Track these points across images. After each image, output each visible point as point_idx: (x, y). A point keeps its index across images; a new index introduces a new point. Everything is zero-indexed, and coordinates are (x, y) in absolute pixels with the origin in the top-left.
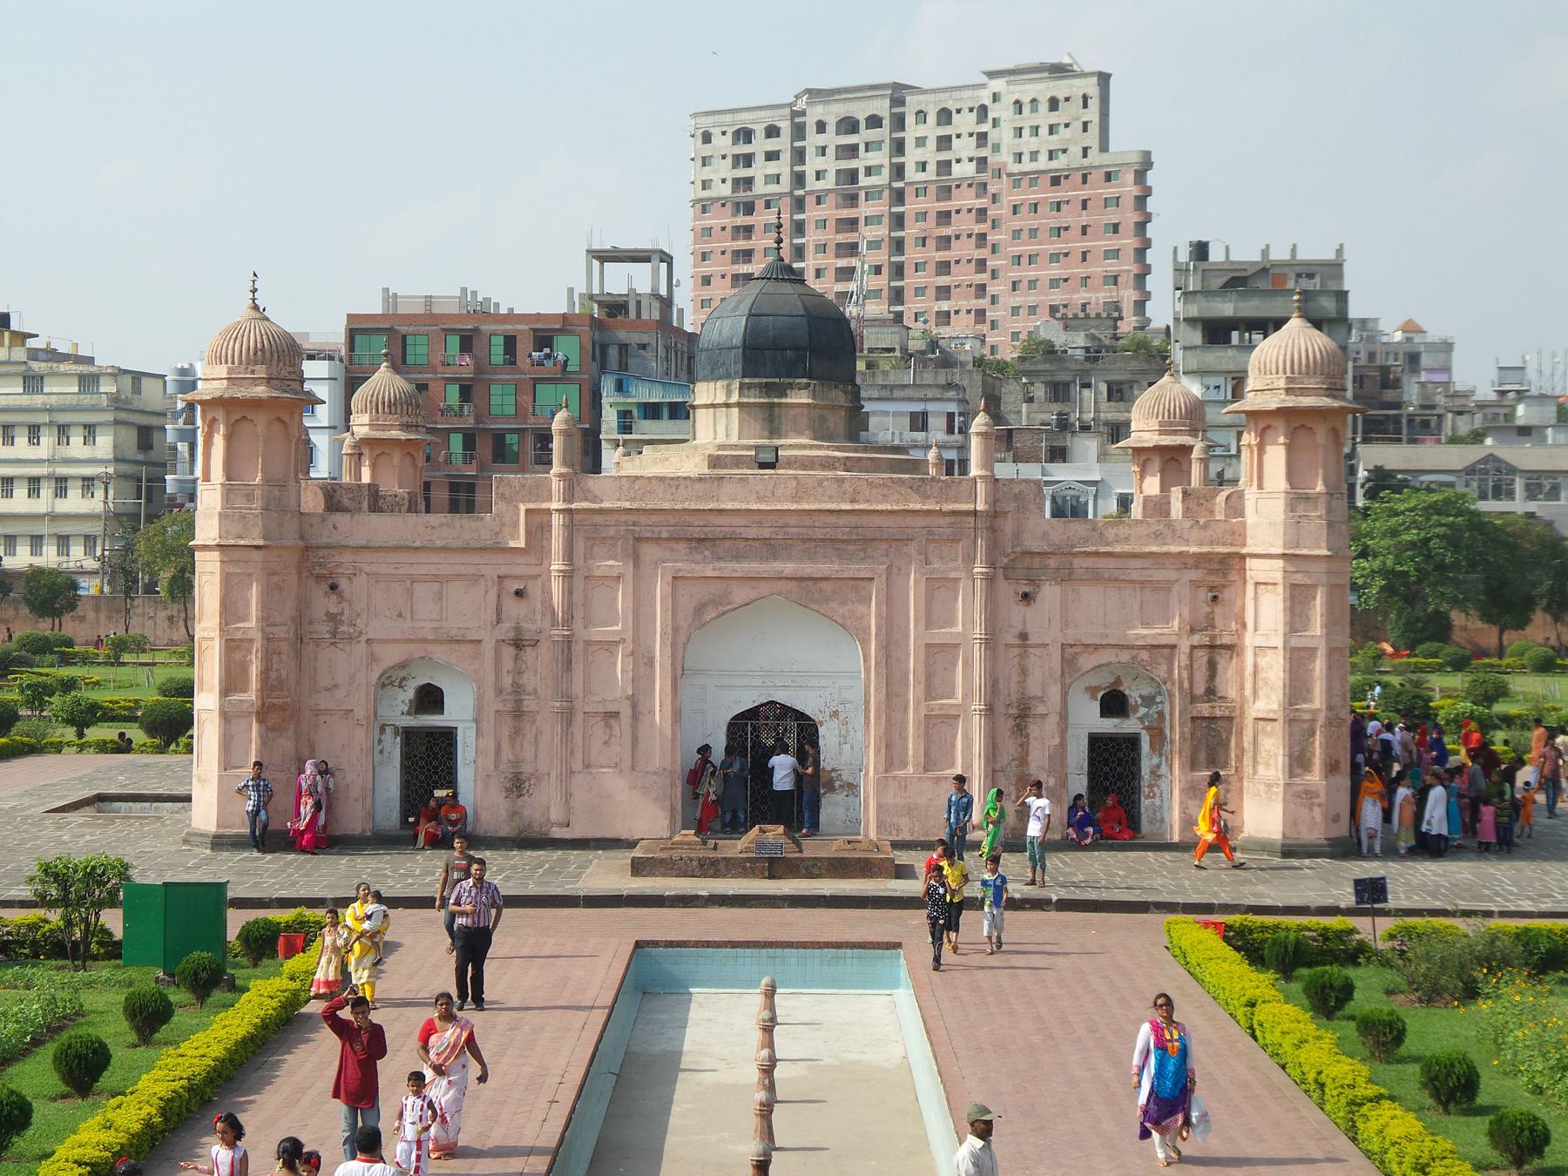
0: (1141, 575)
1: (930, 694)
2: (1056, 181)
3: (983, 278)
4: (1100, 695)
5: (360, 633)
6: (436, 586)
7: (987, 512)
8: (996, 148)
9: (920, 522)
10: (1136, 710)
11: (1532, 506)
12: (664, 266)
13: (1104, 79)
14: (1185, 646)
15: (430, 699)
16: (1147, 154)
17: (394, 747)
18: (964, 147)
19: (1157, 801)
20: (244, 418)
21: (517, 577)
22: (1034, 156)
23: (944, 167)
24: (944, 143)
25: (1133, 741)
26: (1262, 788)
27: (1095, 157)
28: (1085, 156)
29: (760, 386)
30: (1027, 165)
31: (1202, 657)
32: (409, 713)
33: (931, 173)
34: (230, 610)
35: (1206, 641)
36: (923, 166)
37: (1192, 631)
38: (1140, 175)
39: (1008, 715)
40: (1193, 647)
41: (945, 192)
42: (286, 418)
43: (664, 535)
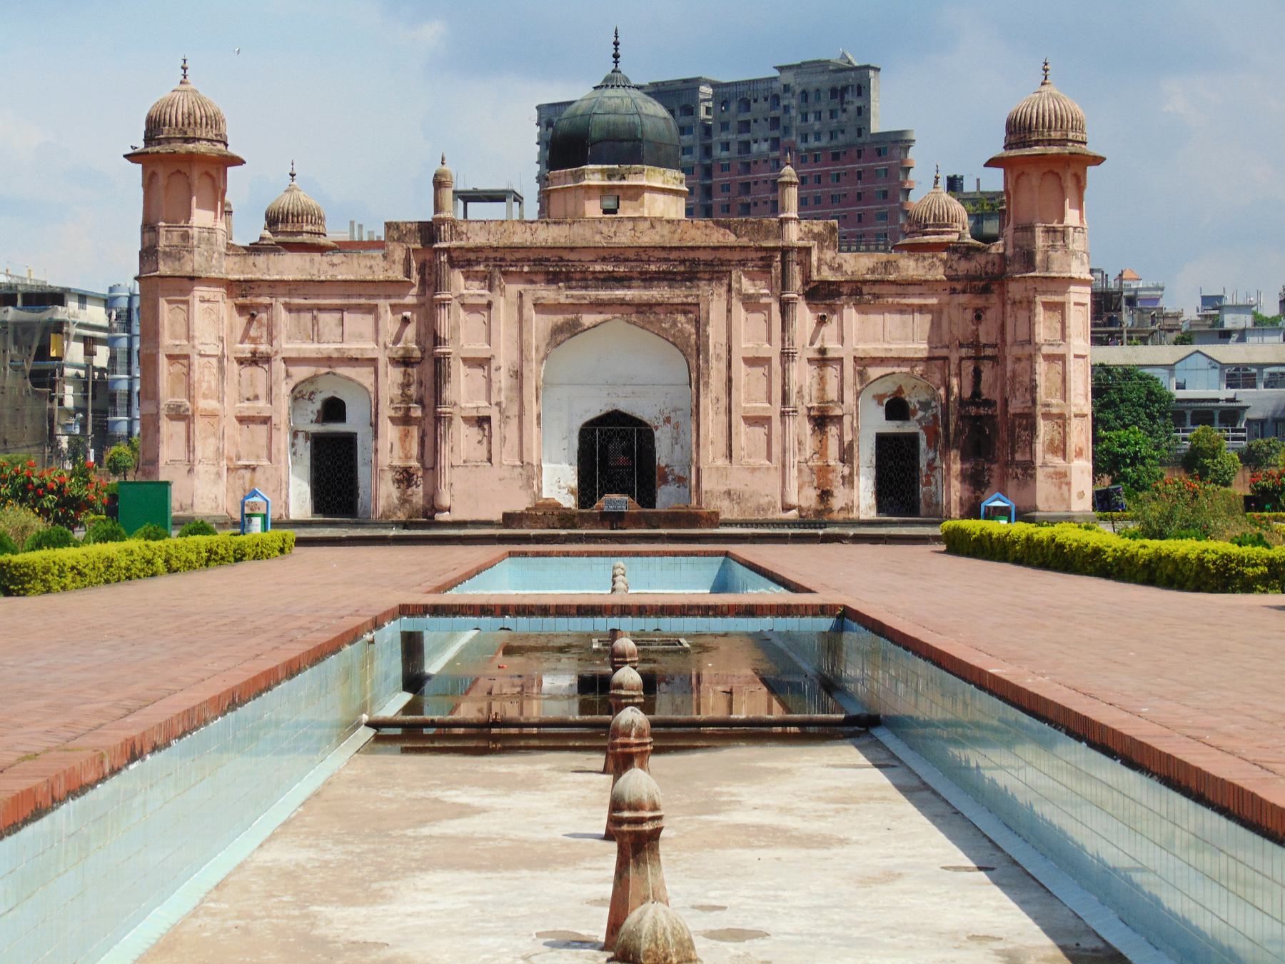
2: (836, 157)
4: (885, 402)
5: (276, 352)
6: (337, 315)
8: (787, 131)
9: (737, 256)
10: (914, 413)
11: (1231, 393)
14: (954, 357)
17: (305, 449)
19: (933, 488)
22: (818, 137)
25: (913, 438)
26: (1019, 471)
28: (860, 135)
29: (602, 171)
30: (813, 143)
31: (968, 367)
32: (317, 421)
35: (972, 352)
36: (726, 146)
37: (961, 346)
39: (810, 418)
40: (961, 359)
41: (747, 168)
42: (213, 173)
43: (526, 269)
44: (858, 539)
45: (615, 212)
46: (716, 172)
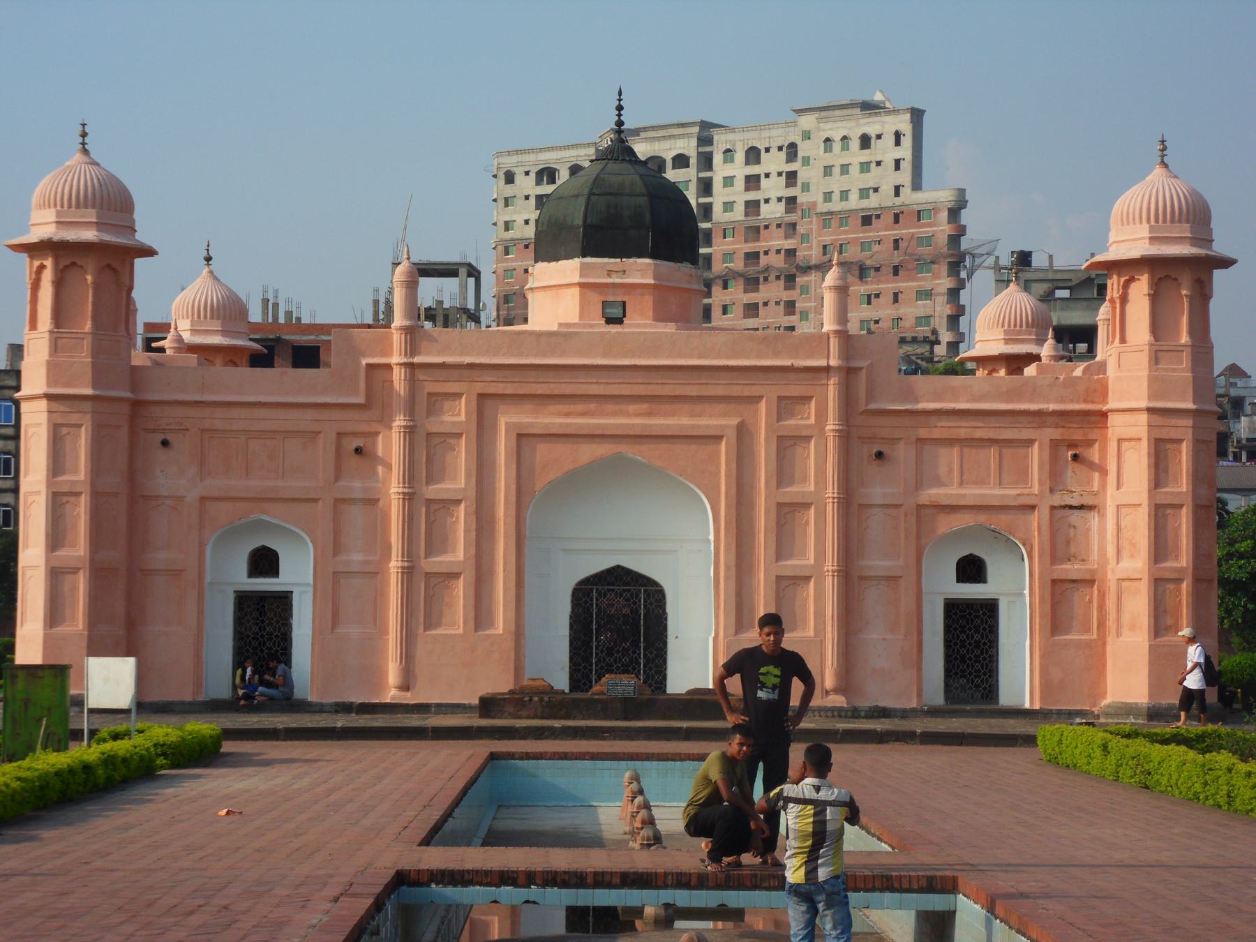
0: (997, 433)
1: (779, 556)
2: (867, 221)
3: (793, 320)
7: (839, 368)
8: (806, 187)
12: (472, 281)
13: (917, 116)
15: (264, 562)
16: (962, 192)
18: (773, 188)
20: (74, 264)
21: (355, 434)
22: (844, 195)
23: (752, 207)
24: (752, 182)
25: (990, 607)
27: (908, 196)
30: (836, 205)
33: (738, 213)
34: (57, 464)
38: (954, 213)
41: (754, 232)
44: (931, 738)
45: (618, 321)
46: (717, 238)
